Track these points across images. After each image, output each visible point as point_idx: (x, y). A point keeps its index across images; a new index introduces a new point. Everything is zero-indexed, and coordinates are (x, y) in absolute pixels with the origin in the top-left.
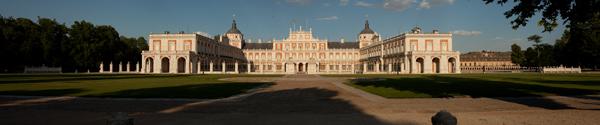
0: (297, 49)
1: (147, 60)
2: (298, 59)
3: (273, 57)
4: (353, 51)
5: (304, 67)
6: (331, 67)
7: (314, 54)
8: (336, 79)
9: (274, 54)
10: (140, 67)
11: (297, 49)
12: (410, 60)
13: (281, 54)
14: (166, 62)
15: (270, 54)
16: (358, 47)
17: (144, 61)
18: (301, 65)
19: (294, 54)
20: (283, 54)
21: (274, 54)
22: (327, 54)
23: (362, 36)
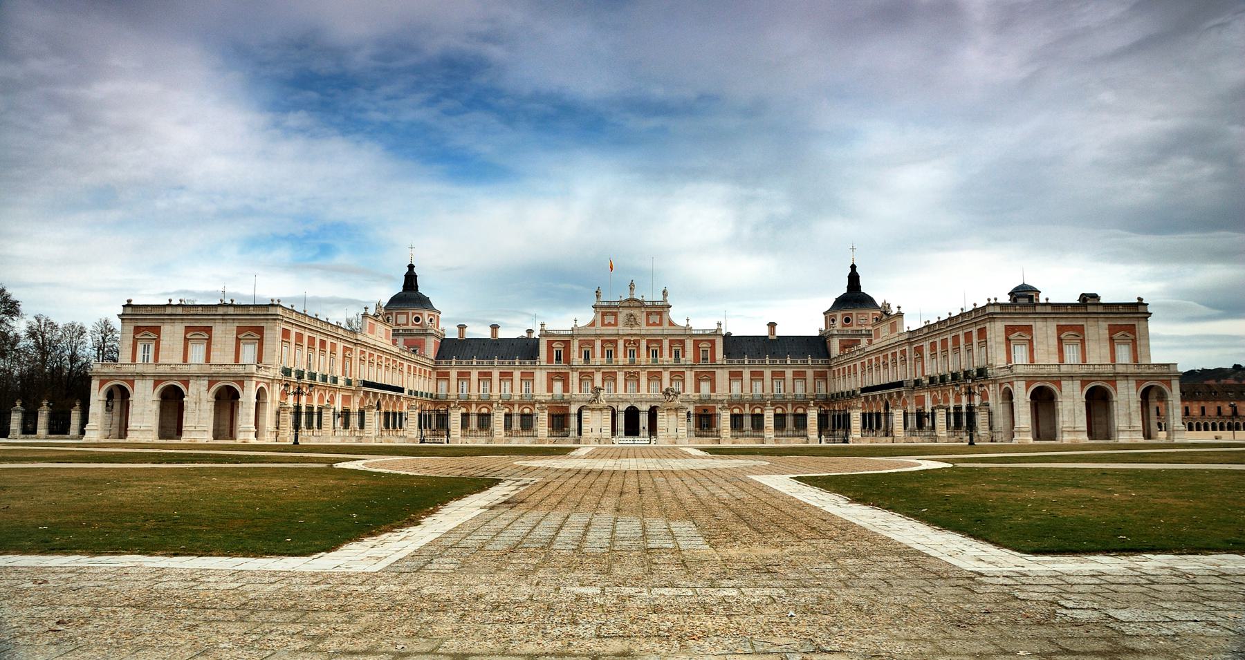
0: (621, 358)
1: (110, 395)
2: (621, 393)
3: (540, 389)
4: (810, 367)
5: (644, 420)
6: (736, 422)
7: (678, 376)
8: (763, 462)
9: (541, 377)
10: (84, 420)
11: (621, 358)
12: (1008, 396)
13: (565, 378)
14: (172, 401)
15: (528, 377)
16: (828, 355)
17: (97, 397)
18: (632, 415)
19: (610, 377)
20: (574, 377)
21: (541, 377)
22: (722, 376)
23: (839, 316)
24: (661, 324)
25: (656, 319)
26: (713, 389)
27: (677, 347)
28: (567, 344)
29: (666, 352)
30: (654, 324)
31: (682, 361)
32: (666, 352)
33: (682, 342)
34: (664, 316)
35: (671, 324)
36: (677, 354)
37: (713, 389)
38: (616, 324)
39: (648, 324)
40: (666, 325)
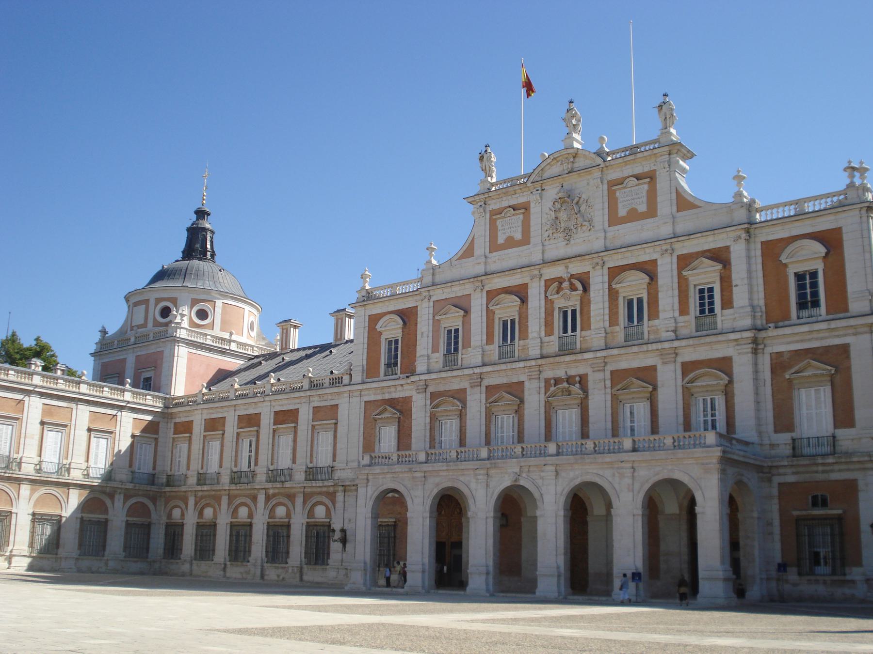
0: (536, 337)
24: (652, 212)
25: (633, 197)
26: (844, 414)
27: (706, 274)
28: (407, 317)
29: (668, 300)
30: (633, 216)
31: (723, 318)
32: (668, 300)
33: (720, 257)
34: (662, 184)
35: (683, 203)
36: (706, 297)
37: (844, 414)
38: (526, 240)
39: (614, 220)
40: (665, 205)
